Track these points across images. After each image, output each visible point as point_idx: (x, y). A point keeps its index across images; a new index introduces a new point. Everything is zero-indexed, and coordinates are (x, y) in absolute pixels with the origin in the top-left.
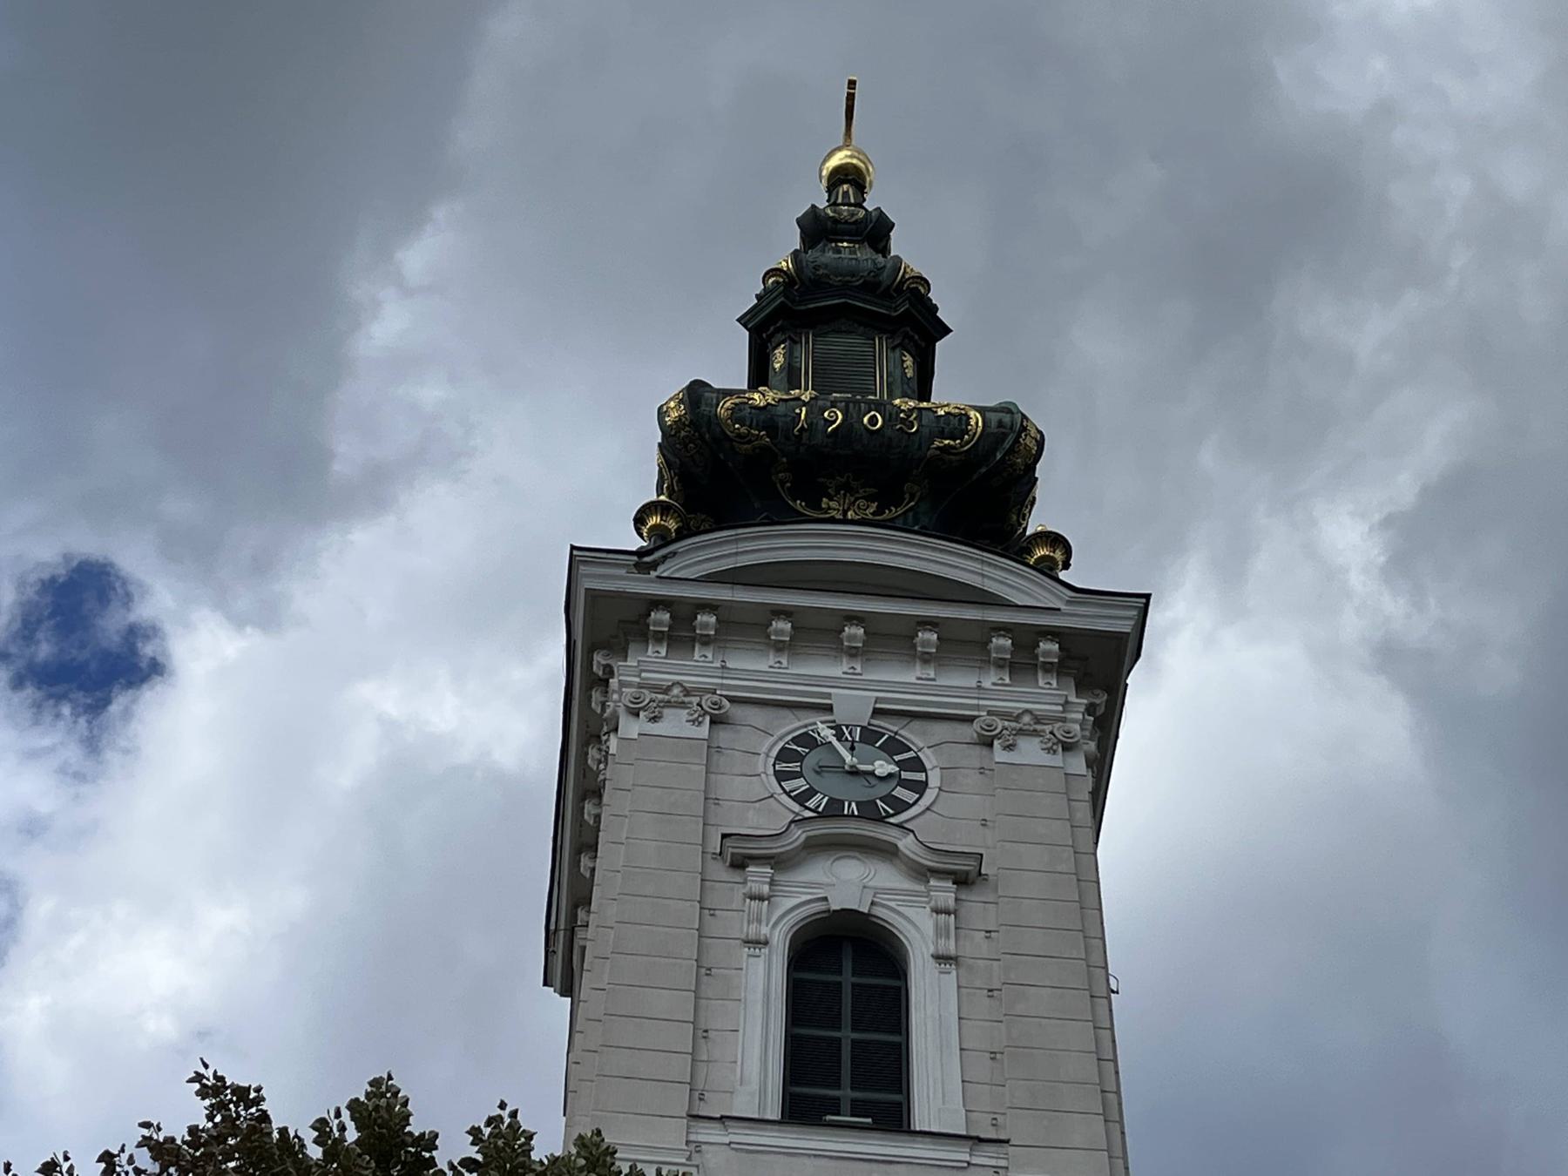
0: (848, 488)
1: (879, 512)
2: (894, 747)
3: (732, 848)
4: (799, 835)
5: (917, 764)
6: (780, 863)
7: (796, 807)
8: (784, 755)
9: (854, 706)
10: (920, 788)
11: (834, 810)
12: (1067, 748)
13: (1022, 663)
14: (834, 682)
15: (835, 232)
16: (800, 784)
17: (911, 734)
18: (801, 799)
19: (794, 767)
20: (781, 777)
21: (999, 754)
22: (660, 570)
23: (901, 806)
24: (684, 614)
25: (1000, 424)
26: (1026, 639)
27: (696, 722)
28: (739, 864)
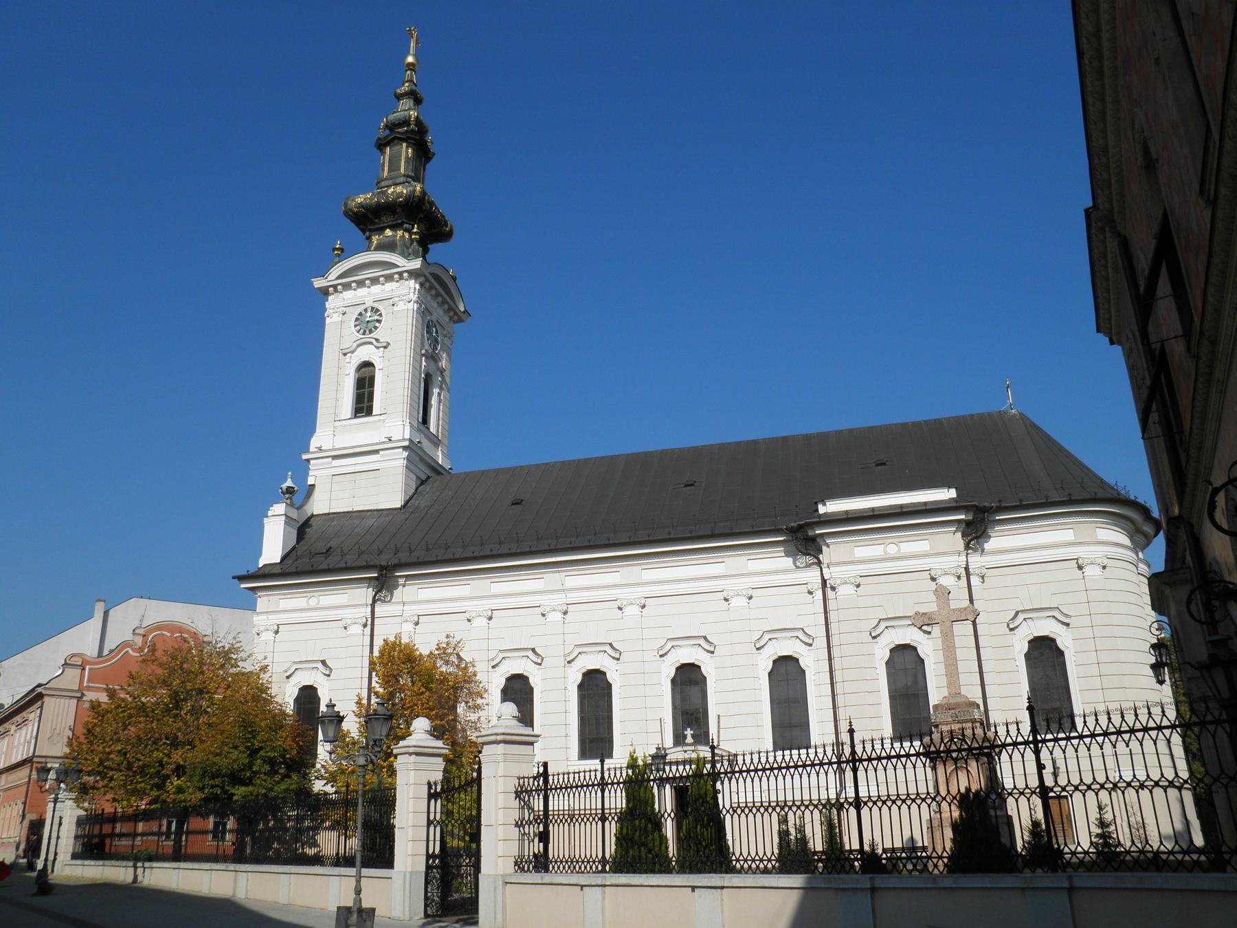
0: (385, 214)
1: (394, 217)
2: (377, 310)
3: (344, 351)
4: (355, 345)
5: (380, 315)
6: (352, 352)
7: (357, 334)
8: (357, 319)
9: (369, 304)
10: (379, 321)
11: (365, 332)
12: (409, 302)
13: (401, 277)
14: (364, 296)
15: (402, 97)
16: (358, 327)
17: (380, 308)
18: (358, 332)
19: (357, 323)
20: (355, 326)
21: (396, 308)
22: (329, 279)
23: (376, 328)
24: (335, 287)
25: (410, 191)
26: (400, 274)
27: (339, 316)
28: (345, 354)
